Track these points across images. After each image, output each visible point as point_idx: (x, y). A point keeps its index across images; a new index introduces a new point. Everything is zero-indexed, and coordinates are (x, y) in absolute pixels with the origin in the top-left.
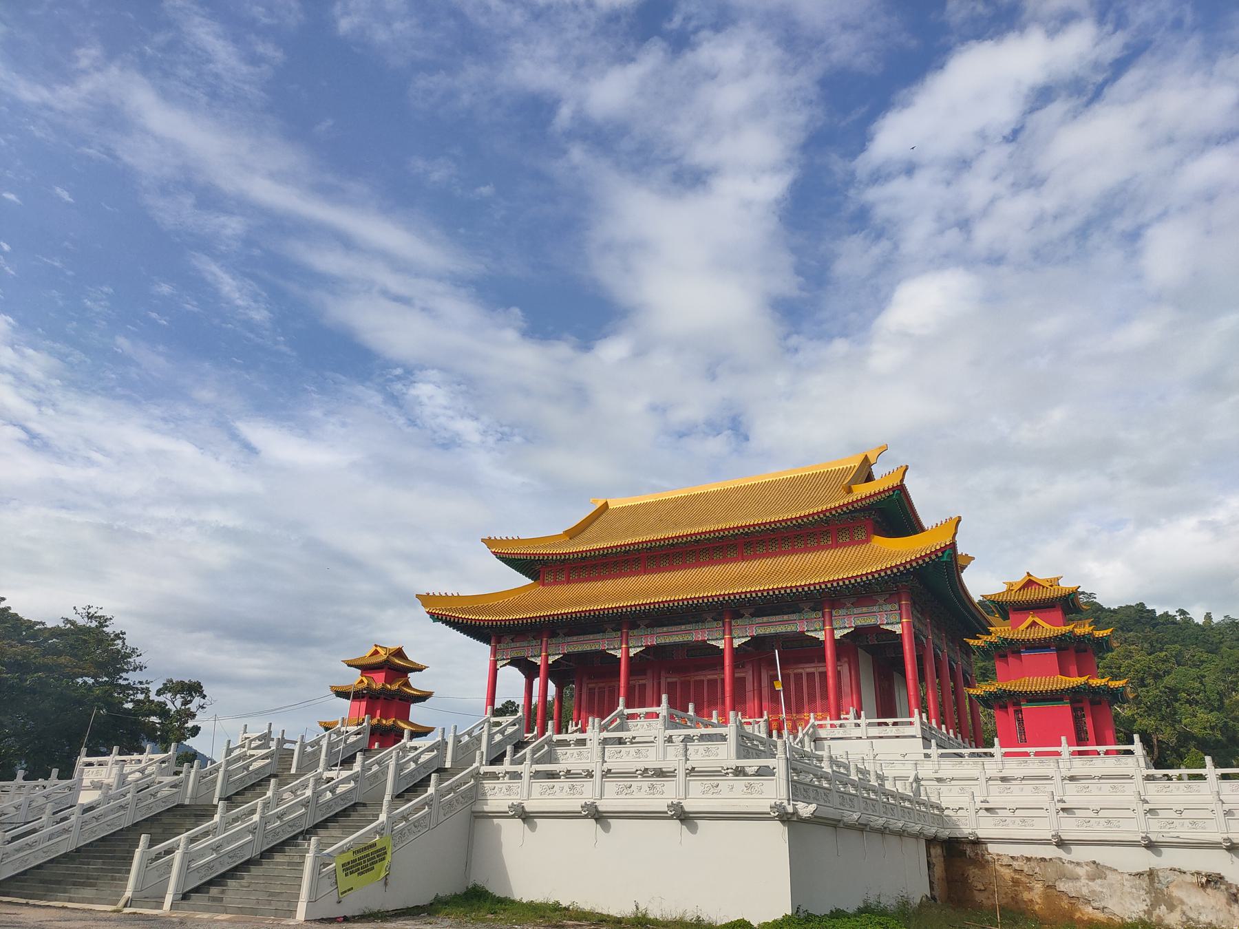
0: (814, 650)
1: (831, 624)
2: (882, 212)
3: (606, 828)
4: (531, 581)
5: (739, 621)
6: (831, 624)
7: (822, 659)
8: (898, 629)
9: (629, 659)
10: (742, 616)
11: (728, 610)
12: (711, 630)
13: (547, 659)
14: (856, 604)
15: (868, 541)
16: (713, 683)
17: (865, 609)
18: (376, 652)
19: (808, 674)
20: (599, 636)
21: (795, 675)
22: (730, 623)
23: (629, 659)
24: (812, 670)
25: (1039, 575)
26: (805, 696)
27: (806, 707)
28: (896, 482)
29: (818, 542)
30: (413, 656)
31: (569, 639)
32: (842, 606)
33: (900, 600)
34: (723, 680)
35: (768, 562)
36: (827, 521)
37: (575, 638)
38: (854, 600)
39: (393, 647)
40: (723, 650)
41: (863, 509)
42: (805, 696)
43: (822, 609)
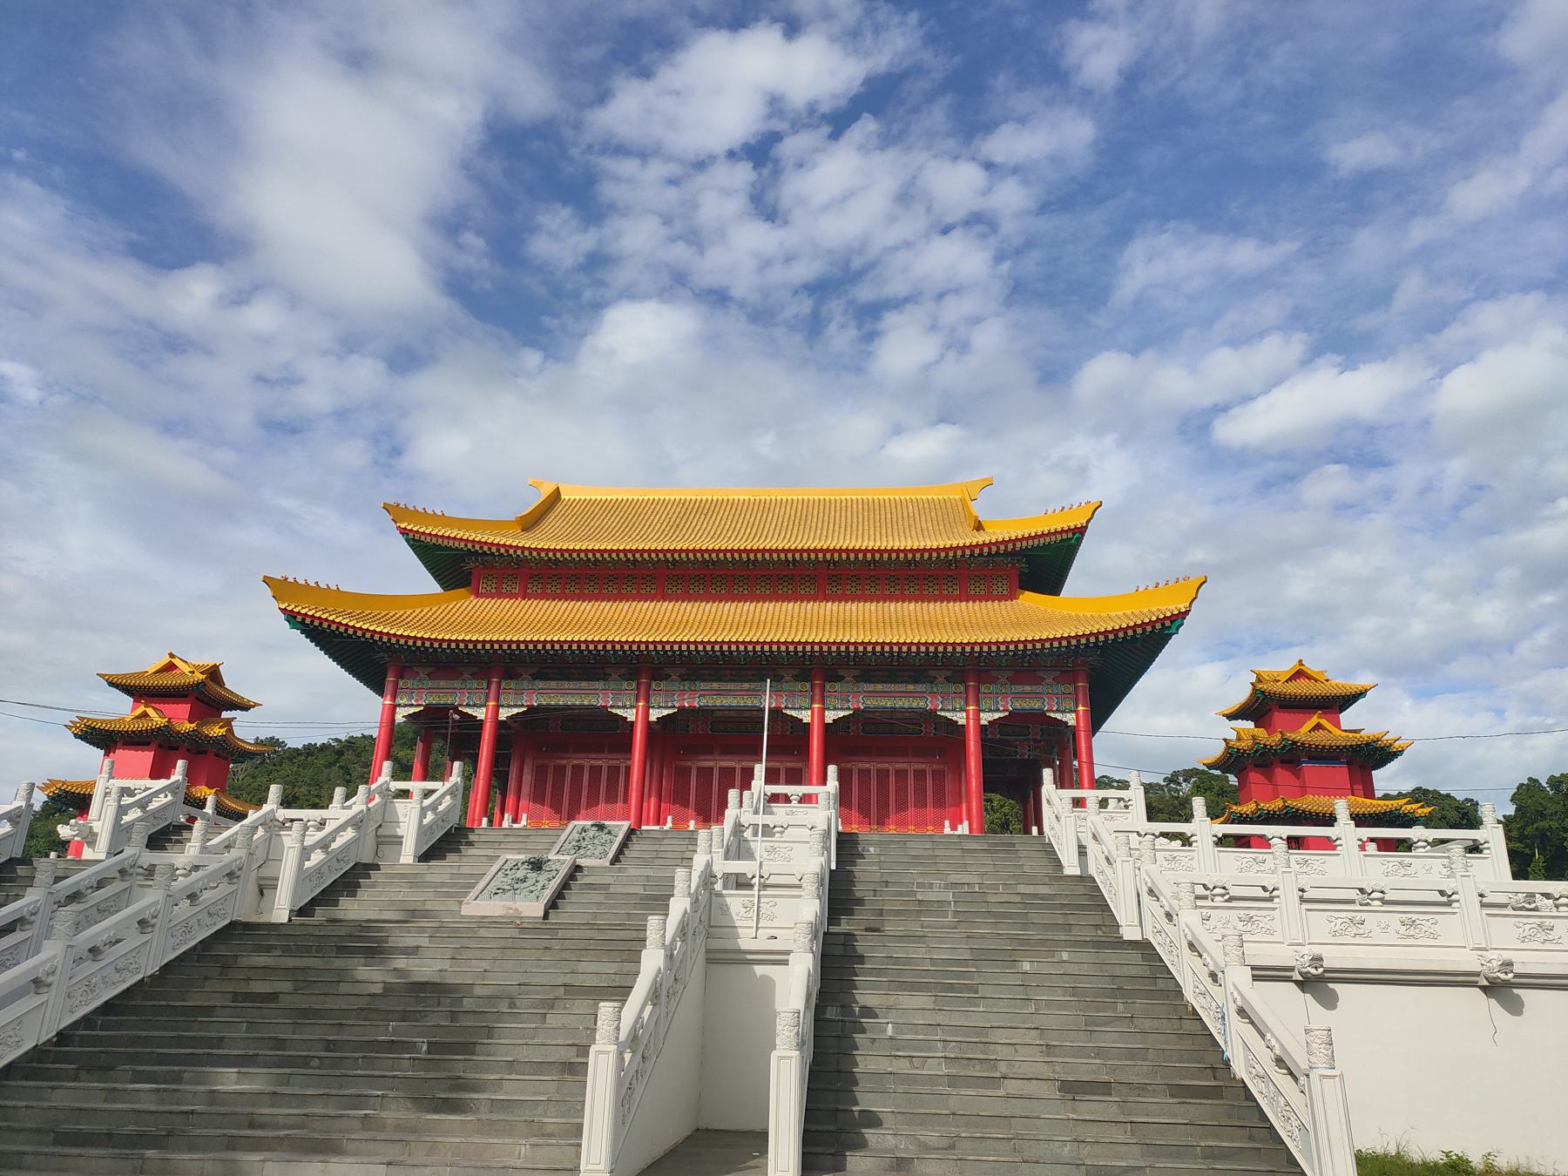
0: (615, 734)
1: (647, 700)
2: (609, 191)
3: (1515, 1007)
4: (433, 587)
5: (838, 686)
6: (497, 700)
7: (628, 748)
8: (1070, 719)
9: (649, 725)
10: (840, 679)
11: (817, 667)
12: (618, 693)
13: (647, 714)
14: (1013, 681)
15: (1012, 596)
16: (614, 771)
17: (1028, 688)
18: (171, 667)
19: (897, 771)
20: (600, 685)
21: (897, 771)
22: (649, 686)
23: (649, 725)
24: (904, 766)
25: (1311, 666)
26: (585, 792)
27: (893, 816)
28: (1079, 522)
29: (620, 589)
30: (234, 683)
31: (540, 684)
32: (994, 681)
33: (1075, 682)
34: (628, 770)
35: (707, 607)
36: (519, 560)
37: (553, 684)
38: (1010, 674)
39: (208, 661)
40: (1074, 729)
41: (1014, 553)
42: (585, 792)
43: (963, 681)
